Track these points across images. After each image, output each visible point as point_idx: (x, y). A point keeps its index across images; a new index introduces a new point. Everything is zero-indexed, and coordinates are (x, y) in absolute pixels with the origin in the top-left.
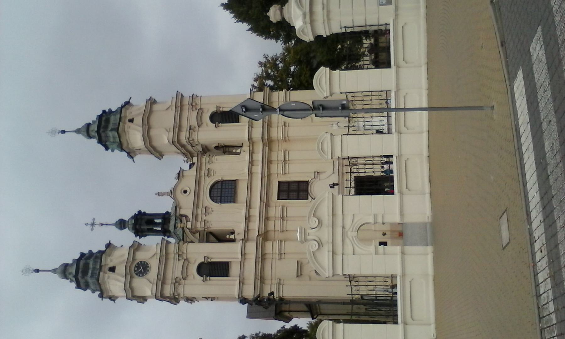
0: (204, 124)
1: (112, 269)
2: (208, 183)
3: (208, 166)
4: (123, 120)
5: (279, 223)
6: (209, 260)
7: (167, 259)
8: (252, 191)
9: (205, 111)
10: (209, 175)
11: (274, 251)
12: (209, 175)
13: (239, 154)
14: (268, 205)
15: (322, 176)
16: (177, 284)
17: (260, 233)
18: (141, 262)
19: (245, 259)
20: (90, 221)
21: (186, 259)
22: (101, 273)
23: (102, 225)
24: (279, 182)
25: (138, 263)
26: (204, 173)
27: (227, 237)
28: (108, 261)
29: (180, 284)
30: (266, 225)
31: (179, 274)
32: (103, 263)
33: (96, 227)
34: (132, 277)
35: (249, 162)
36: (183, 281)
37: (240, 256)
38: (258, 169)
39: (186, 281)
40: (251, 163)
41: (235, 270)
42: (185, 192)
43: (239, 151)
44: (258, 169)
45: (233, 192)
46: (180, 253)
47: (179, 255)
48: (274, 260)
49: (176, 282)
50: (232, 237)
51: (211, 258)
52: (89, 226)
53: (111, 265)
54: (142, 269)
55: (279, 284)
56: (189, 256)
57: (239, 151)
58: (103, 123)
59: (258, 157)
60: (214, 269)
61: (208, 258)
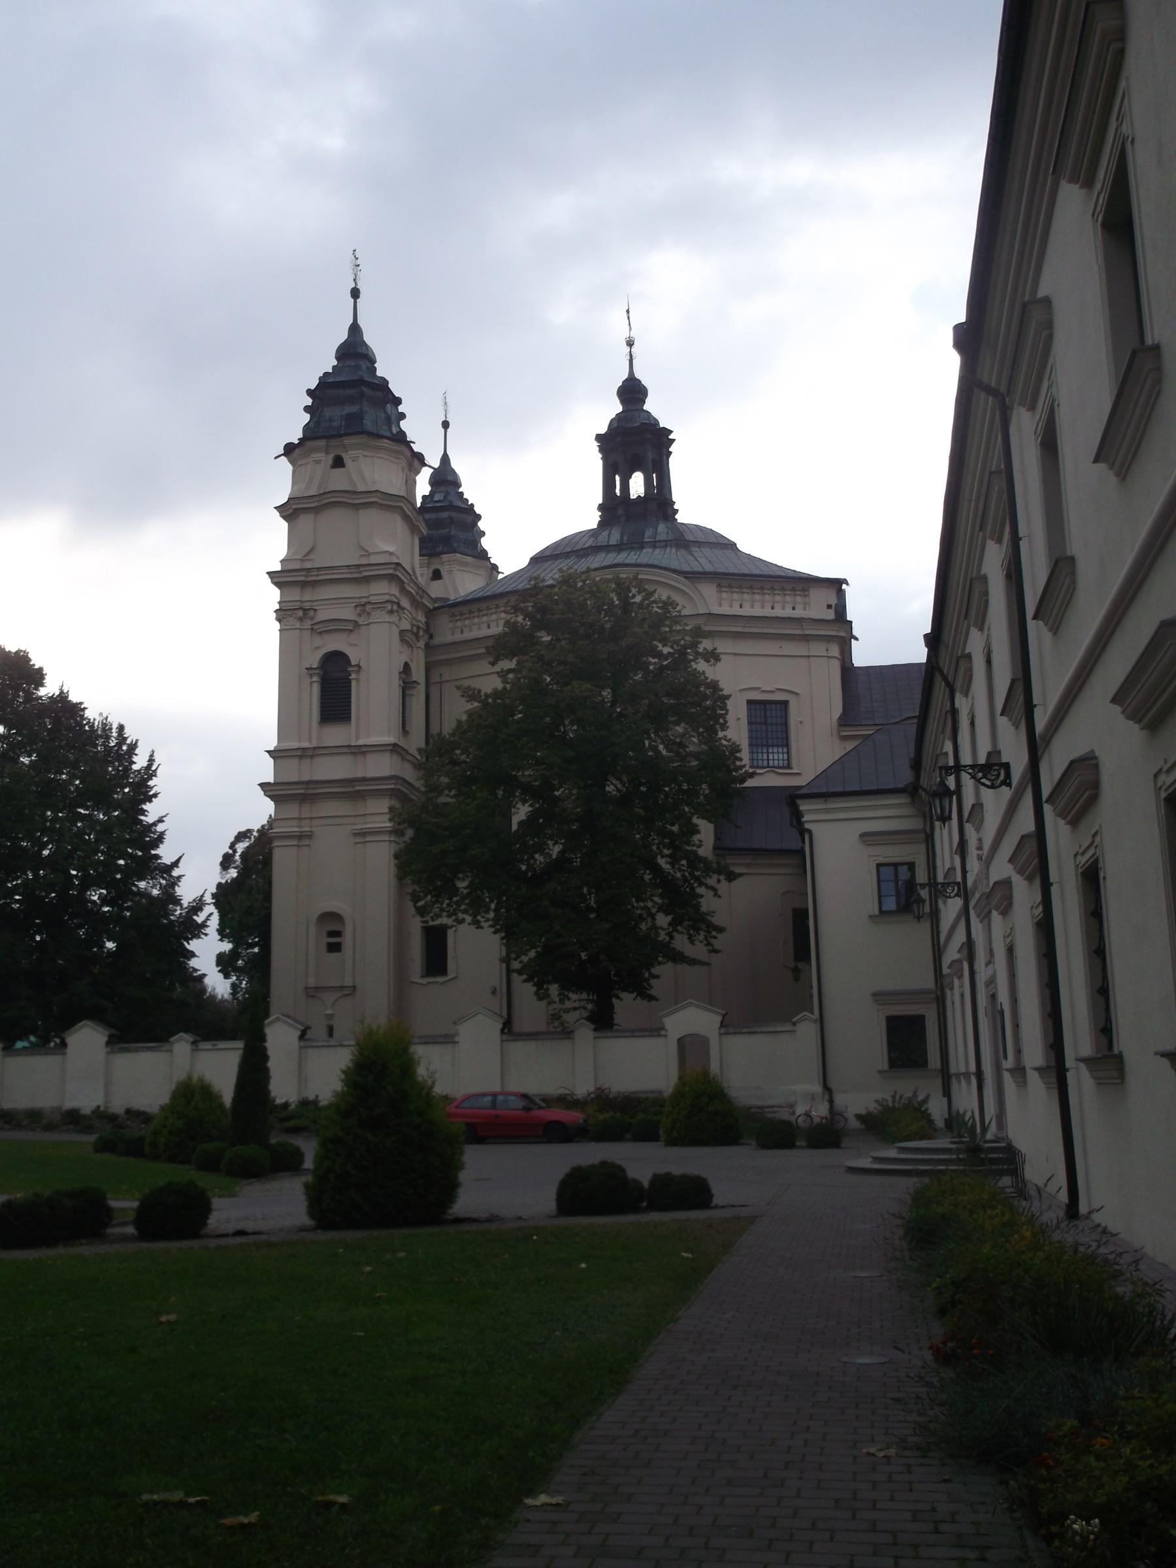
16: (300, 613)
19: (354, 754)
21: (357, 625)
22: (322, 443)
29: (301, 619)
31: (324, 614)
32: (347, 441)
36: (308, 624)
37: (361, 742)
39: (307, 634)
41: (335, 735)
46: (368, 607)
47: (363, 607)
49: (305, 610)
51: (357, 680)
53: (347, 458)
55: (300, 837)
61: (358, 672)
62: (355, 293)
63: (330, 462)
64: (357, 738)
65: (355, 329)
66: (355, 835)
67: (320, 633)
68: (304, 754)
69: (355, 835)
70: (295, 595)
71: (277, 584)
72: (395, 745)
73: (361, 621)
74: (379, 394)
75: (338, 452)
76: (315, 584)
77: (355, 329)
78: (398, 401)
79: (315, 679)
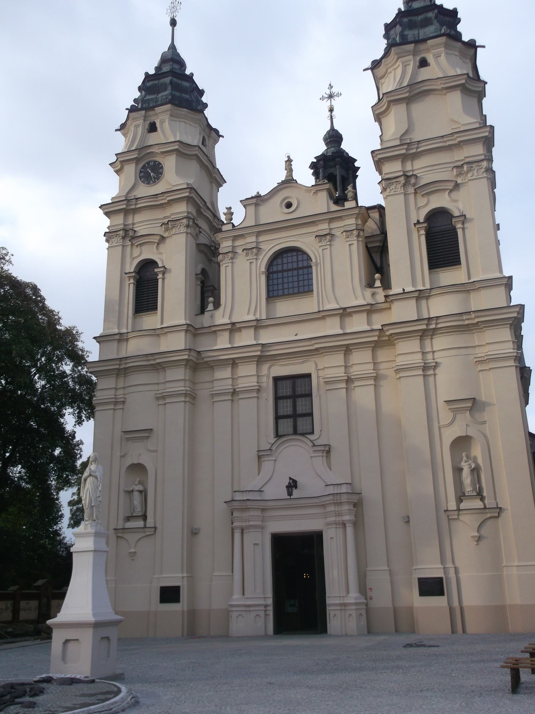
0: (422, 201)
1: (153, 128)
2: (304, 240)
3: (337, 232)
4: (422, 46)
5: (227, 385)
6: (160, 276)
7: (161, 206)
8: (295, 324)
9: (454, 195)
10: (320, 237)
11: (168, 385)
12: (320, 237)
13: (370, 284)
14: (260, 360)
15: (319, 462)
17: (203, 355)
18: (162, 168)
19: (158, 335)
20: (334, 90)
23: (331, 110)
24: (308, 376)
25: (160, 163)
26: (324, 227)
27: (211, 299)
28: (161, 117)
30: (223, 363)
33: (327, 104)
34: (137, 160)
35: (345, 309)
38: (332, 327)
40: (345, 313)
42: (289, 205)
43: (378, 284)
44: (332, 327)
45: (291, 291)
48: (155, 387)
50: (210, 307)
52: (328, 92)
54: (150, 171)
56: (168, 241)
57: (378, 284)
58: (420, 18)
59: (358, 324)
60: (144, 287)
61: (164, 273)
62: (173, 23)
63: (147, 127)
64: (162, 323)
65: (173, 47)
66: (158, 399)
67: (137, 246)
68: (121, 338)
69: (158, 399)
70: (119, 220)
71: (107, 214)
72: (188, 325)
73: (165, 235)
74: (186, 84)
75: (152, 119)
76: (136, 211)
77: (173, 47)
78: (201, 93)
79: (132, 281)
